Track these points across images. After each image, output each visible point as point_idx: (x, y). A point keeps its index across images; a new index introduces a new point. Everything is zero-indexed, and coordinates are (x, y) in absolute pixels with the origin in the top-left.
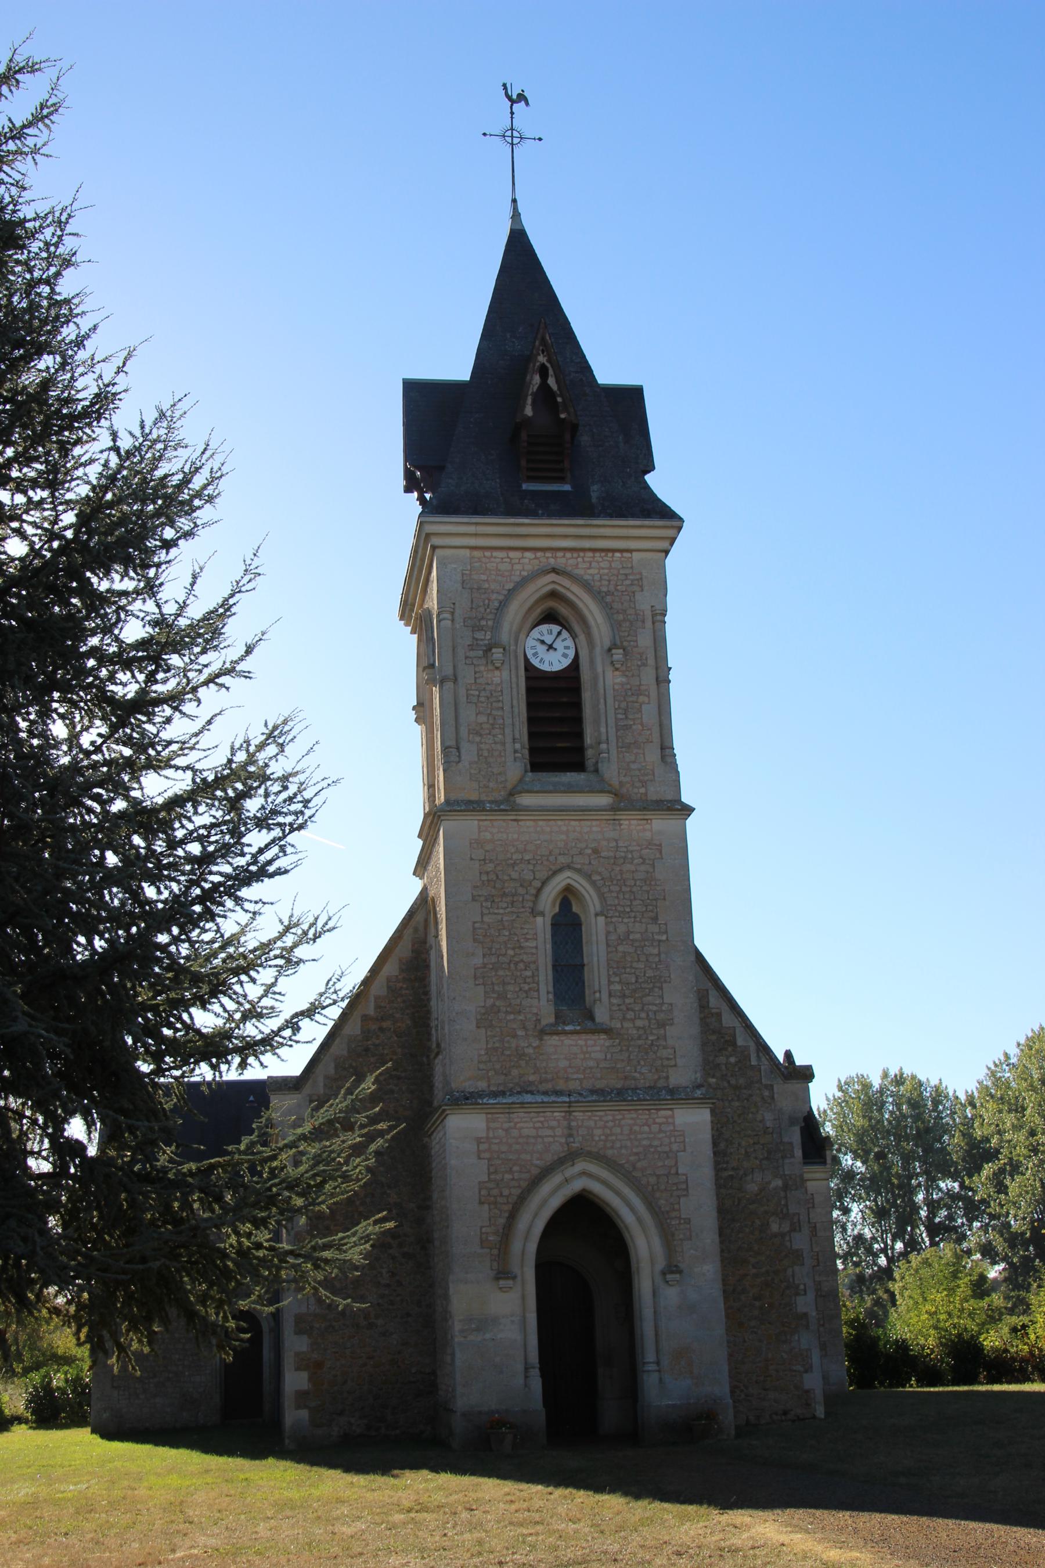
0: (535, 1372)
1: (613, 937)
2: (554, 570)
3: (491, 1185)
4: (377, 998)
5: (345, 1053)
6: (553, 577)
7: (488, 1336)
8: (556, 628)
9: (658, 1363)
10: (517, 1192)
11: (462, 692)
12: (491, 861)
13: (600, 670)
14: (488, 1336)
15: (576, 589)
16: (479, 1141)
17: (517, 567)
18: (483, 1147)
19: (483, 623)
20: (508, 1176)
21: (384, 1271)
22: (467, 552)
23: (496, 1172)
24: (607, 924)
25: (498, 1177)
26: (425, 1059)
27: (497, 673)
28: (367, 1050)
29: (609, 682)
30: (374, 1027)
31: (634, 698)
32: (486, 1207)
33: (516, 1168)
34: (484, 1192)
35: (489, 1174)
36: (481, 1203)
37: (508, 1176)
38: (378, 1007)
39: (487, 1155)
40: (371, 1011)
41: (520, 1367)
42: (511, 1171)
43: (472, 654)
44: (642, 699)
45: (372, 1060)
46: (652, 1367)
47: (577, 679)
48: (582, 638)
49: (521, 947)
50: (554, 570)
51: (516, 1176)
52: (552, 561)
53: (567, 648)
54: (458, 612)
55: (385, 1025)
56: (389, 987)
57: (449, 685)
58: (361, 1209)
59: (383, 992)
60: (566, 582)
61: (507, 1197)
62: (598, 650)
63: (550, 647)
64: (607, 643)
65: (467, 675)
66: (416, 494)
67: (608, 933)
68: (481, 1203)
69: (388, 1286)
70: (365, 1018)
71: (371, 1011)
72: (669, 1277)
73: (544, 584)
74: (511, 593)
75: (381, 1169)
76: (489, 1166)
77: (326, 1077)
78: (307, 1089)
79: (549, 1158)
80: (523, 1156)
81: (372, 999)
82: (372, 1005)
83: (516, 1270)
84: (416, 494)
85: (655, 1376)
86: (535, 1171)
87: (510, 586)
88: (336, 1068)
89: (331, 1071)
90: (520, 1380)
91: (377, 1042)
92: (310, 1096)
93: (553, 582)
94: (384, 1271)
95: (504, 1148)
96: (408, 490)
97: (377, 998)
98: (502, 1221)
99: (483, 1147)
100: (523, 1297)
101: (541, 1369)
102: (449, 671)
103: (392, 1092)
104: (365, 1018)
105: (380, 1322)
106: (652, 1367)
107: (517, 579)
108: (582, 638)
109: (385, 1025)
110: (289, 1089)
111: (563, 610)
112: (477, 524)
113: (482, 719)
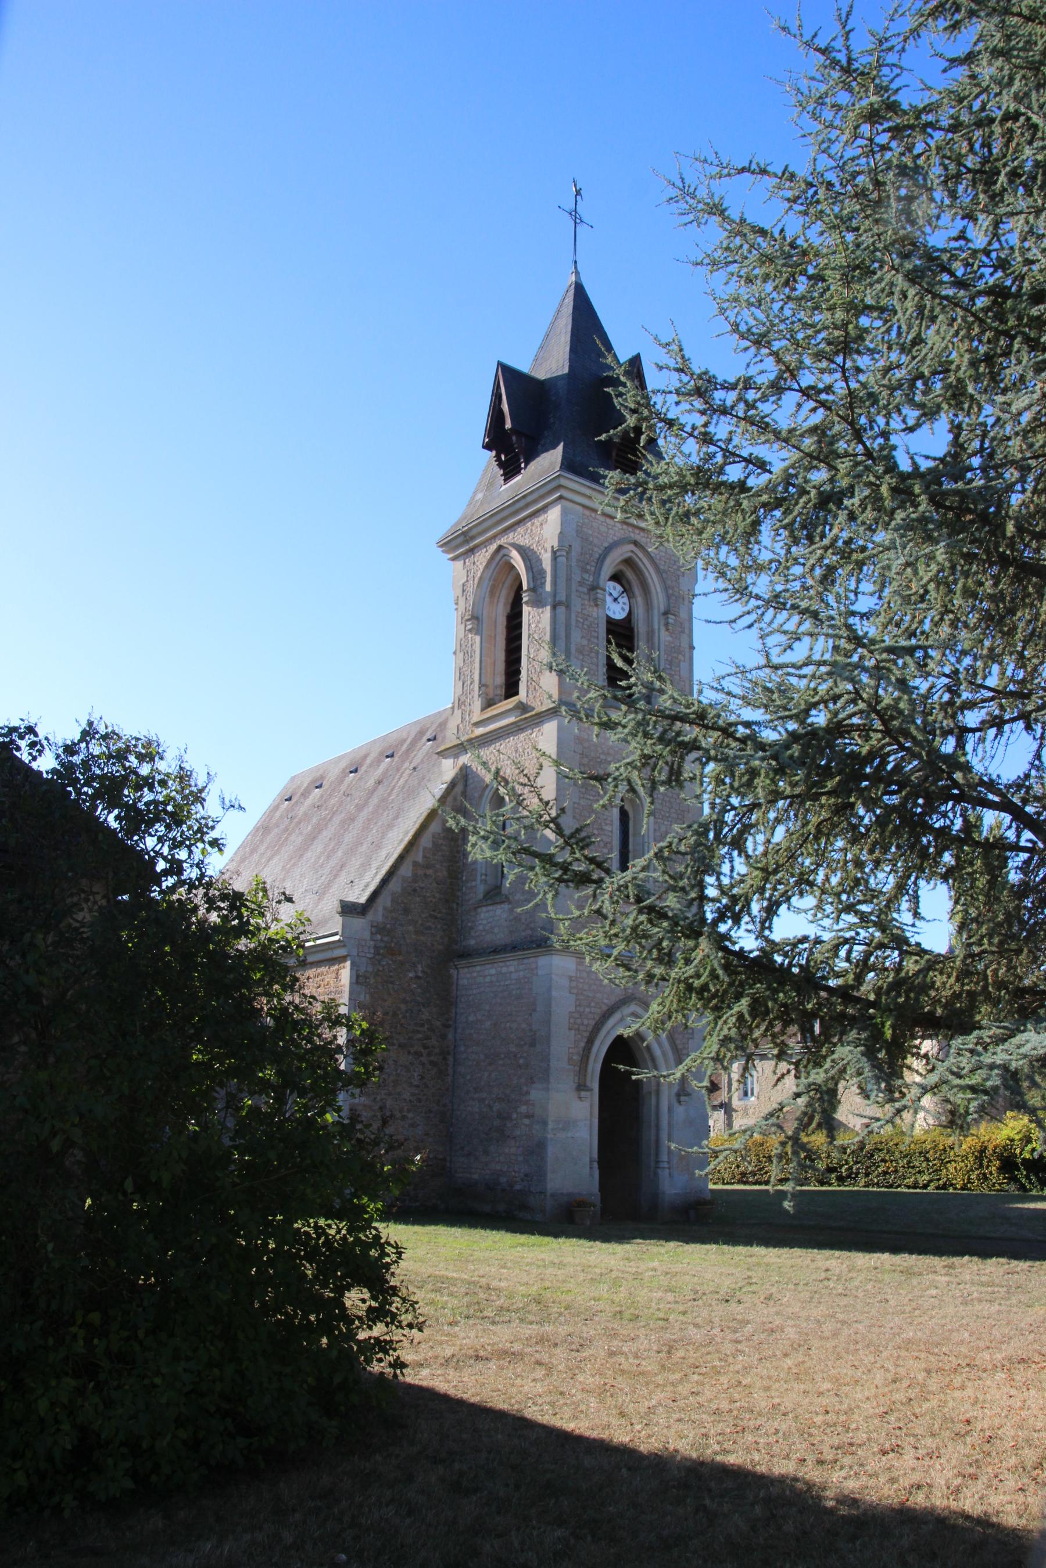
0: (596, 1165)
1: (658, 834)
2: (636, 543)
3: (577, 1015)
4: (425, 849)
5: (399, 890)
6: (632, 547)
7: (569, 1135)
8: (619, 588)
9: (668, 1162)
10: (593, 1023)
11: (573, 617)
12: (587, 756)
13: (656, 627)
14: (569, 1135)
15: (645, 561)
16: (570, 978)
17: (611, 531)
18: (574, 984)
19: (588, 567)
20: (587, 1010)
21: (416, 1074)
22: (580, 509)
23: (580, 1005)
24: (655, 823)
25: (582, 1009)
26: (455, 906)
27: (595, 609)
28: (415, 890)
29: (662, 638)
30: (420, 872)
31: (675, 655)
32: (573, 1032)
33: (593, 1004)
34: (572, 1020)
35: (576, 1006)
36: (570, 1029)
37: (587, 1010)
38: (424, 857)
39: (575, 991)
40: (420, 858)
41: (588, 1159)
42: (589, 1006)
43: (580, 589)
44: (681, 657)
45: (418, 899)
46: (666, 1165)
47: (631, 630)
48: (640, 599)
49: (602, 829)
50: (636, 543)
51: (593, 1010)
52: (632, 535)
53: (624, 604)
54: (573, 554)
55: (430, 872)
56: (433, 842)
57: (561, 610)
58: (403, 1021)
59: (429, 845)
60: (641, 555)
61: (587, 1026)
62: (656, 612)
63: (615, 600)
64: (662, 609)
65: (577, 604)
66: (494, 453)
67: (655, 830)
68: (570, 1029)
69: (417, 1086)
70: (415, 864)
71: (420, 858)
72: (682, 1098)
73: (625, 551)
74: (608, 550)
75: (419, 990)
76: (577, 1000)
77: (385, 908)
78: (370, 916)
79: (614, 999)
80: (598, 995)
81: (421, 850)
82: (421, 854)
83: (588, 1084)
84: (494, 453)
85: (667, 1171)
86: (605, 1008)
87: (606, 545)
88: (392, 901)
89: (389, 904)
90: (587, 1170)
91: (422, 885)
92: (372, 922)
93: (632, 551)
94: (416, 1074)
95: (586, 987)
96: (487, 447)
97: (425, 849)
98: (582, 1044)
99: (574, 984)
100: (591, 1106)
101: (600, 1163)
102: (562, 596)
103: (430, 928)
104: (415, 864)
105: (410, 1115)
106: (666, 1165)
107: (611, 541)
108: (640, 599)
109: (430, 872)
110: (358, 913)
111: (630, 574)
112: (594, 489)
113: (585, 642)
